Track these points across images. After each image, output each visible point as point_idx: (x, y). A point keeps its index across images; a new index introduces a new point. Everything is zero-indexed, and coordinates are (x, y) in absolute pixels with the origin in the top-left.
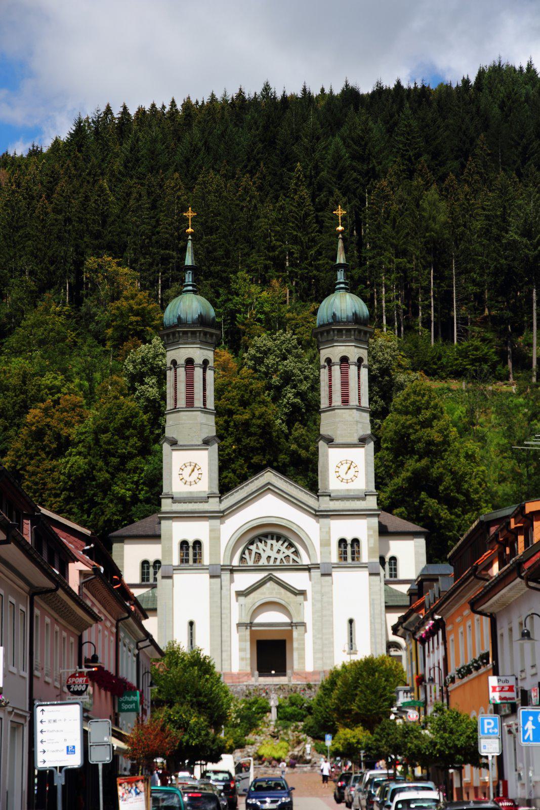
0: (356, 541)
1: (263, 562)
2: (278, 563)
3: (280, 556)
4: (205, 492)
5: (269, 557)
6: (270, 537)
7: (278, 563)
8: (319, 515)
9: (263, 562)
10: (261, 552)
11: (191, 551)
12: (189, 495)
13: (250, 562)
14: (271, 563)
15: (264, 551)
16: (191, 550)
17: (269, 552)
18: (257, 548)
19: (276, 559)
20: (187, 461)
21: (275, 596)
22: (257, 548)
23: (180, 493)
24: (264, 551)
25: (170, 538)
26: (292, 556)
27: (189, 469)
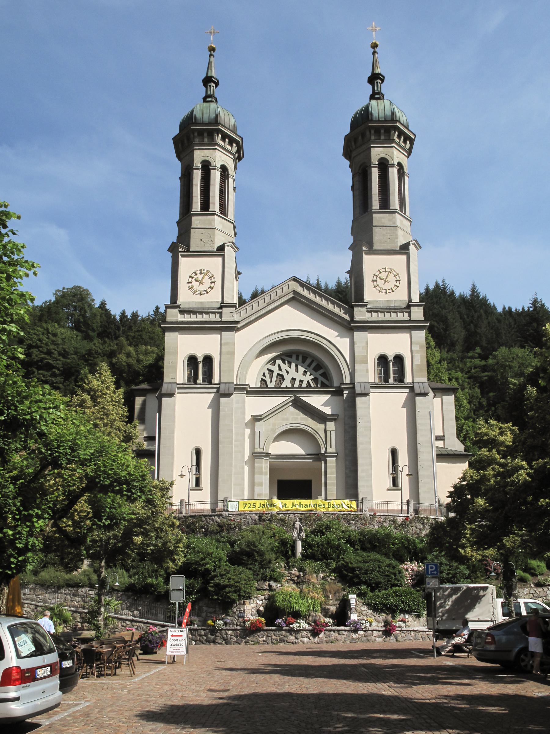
0: (399, 359)
1: (287, 383)
2: (304, 384)
4: (218, 302)
5: (294, 379)
6: (294, 357)
9: (287, 383)
10: (284, 373)
12: (200, 306)
14: (297, 384)
15: (288, 372)
16: (201, 366)
18: (280, 369)
19: (301, 381)
20: (197, 269)
21: (299, 422)
22: (280, 369)
23: (189, 303)
24: (288, 372)
25: (175, 353)
26: (321, 379)
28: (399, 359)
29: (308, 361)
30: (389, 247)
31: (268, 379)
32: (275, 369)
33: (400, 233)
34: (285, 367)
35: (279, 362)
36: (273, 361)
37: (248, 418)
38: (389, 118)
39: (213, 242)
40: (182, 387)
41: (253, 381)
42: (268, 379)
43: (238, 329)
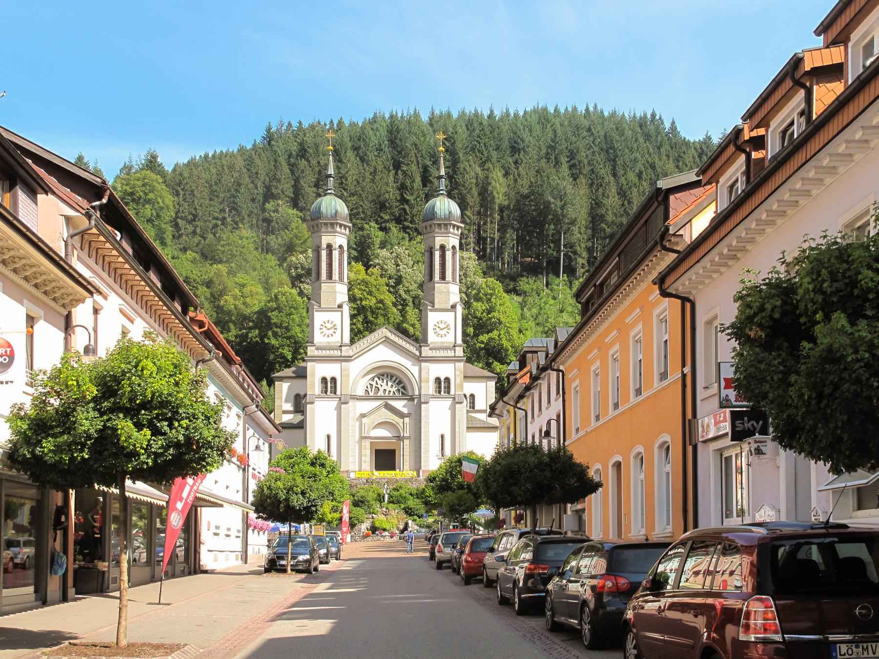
0: (447, 380)
1: (381, 393)
2: (391, 394)
3: (394, 389)
7: (391, 394)
8: (419, 359)
9: (381, 393)
10: (379, 386)
11: (329, 385)
13: (372, 394)
17: (385, 387)
20: (326, 320)
25: (313, 376)
26: (401, 390)
27: (330, 324)
28: (447, 380)
29: (394, 379)
30: (444, 306)
31: (369, 390)
32: (374, 383)
33: (451, 296)
34: (380, 382)
35: (376, 379)
36: (373, 379)
37: (358, 415)
38: (447, 216)
39: (335, 301)
40: (319, 397)
41: (360, 392)
42: (369, 390)
43: (352, 360)
